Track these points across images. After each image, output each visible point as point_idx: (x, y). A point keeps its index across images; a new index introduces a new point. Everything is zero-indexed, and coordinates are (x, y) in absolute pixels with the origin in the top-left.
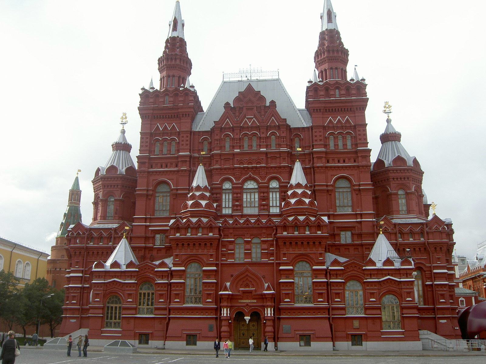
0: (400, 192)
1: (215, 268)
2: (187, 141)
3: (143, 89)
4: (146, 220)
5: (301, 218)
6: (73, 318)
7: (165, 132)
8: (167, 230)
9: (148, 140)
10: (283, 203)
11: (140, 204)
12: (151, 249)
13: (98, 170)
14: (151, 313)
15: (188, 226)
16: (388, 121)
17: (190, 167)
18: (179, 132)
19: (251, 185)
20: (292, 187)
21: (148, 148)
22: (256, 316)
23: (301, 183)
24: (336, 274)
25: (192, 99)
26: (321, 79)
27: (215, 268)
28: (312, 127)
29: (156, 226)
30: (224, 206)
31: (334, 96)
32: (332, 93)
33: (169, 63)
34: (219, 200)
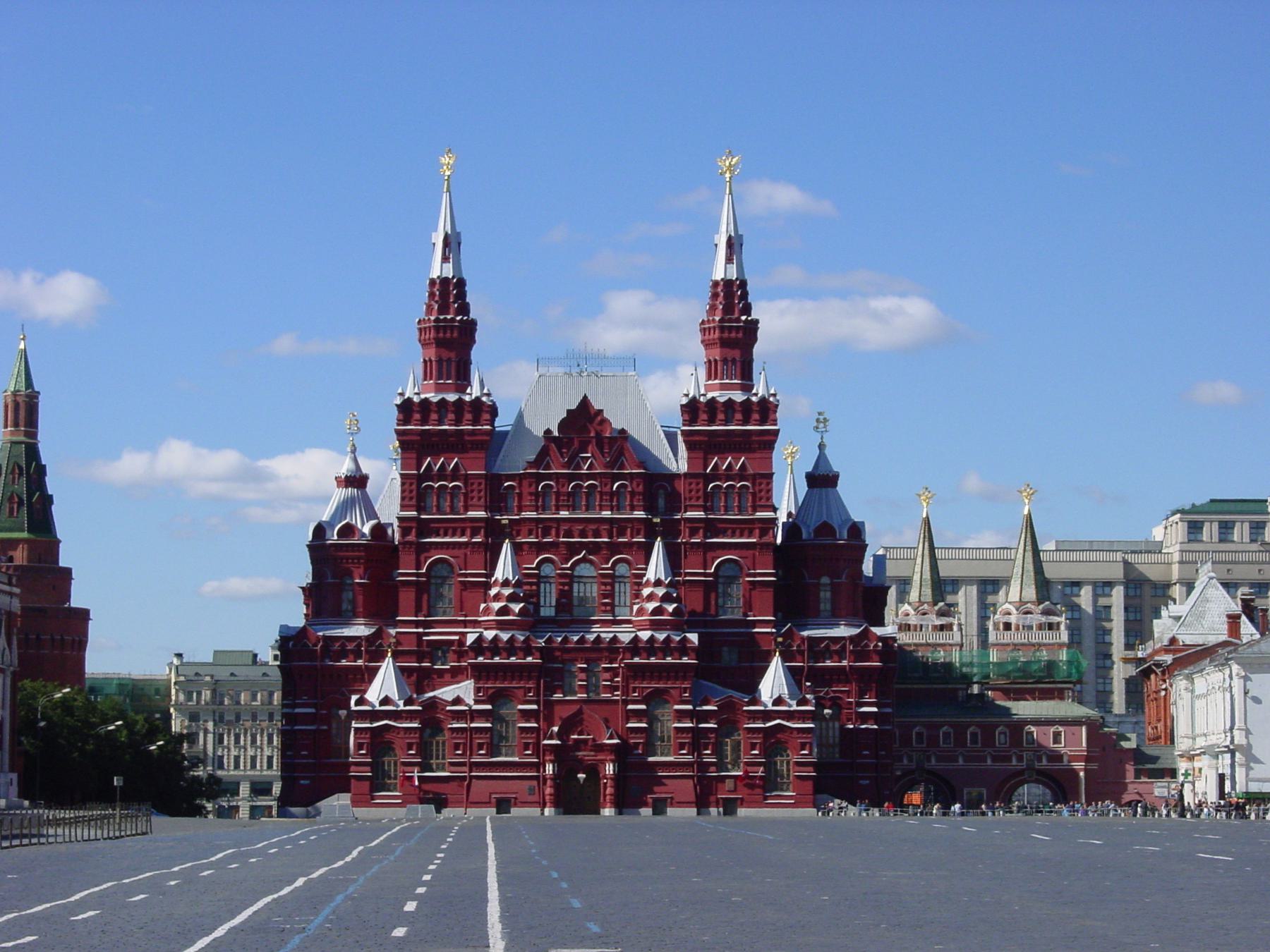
0: (825, 580)
1: (535, 707)
2: (480, 491)
3: (402, 394)
4: (417, 624)
5: (661, 636)
6: (304, 778)
7: (442, 474)
8: (452, 642)
9: (414, 487)
10: (636, 607)
11: (407, 598)
12: (429, 671)
13: (320, 530)
14: (443, 770)
15: (495, 647)
16: (821, 447)
17: (486, 536)
18: (467, 475)
19: (585, 570)
20: (648, 583)
21: (414, 502)
22: (594, 772)
23: (663, 578)
24: (706, 716)
25: (487, 416)
26: (702, 392)
27: (535, 707)
28: (685, 475)
29: (436, 635)
30: (542, 603)
31: (726, 423)
32: (721, 416)
33: (441, 335)
34: (537, 594)
